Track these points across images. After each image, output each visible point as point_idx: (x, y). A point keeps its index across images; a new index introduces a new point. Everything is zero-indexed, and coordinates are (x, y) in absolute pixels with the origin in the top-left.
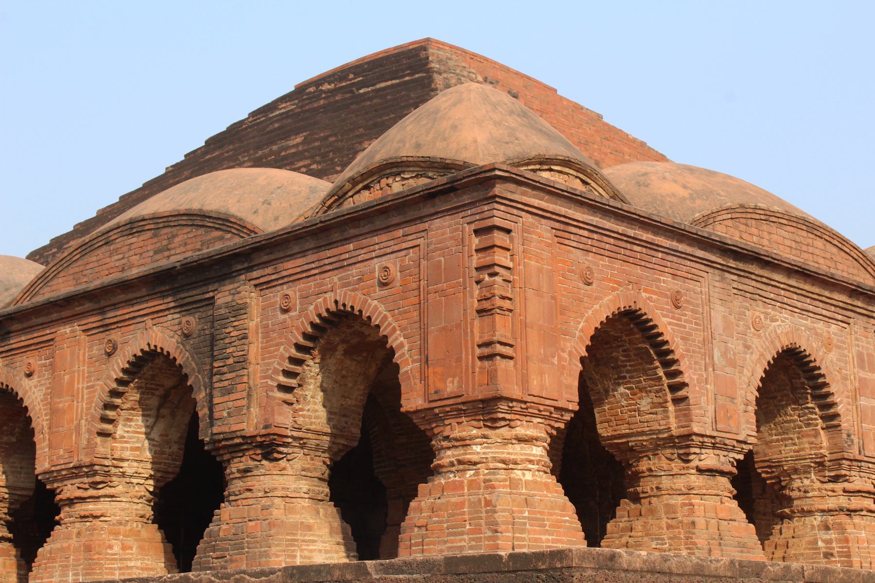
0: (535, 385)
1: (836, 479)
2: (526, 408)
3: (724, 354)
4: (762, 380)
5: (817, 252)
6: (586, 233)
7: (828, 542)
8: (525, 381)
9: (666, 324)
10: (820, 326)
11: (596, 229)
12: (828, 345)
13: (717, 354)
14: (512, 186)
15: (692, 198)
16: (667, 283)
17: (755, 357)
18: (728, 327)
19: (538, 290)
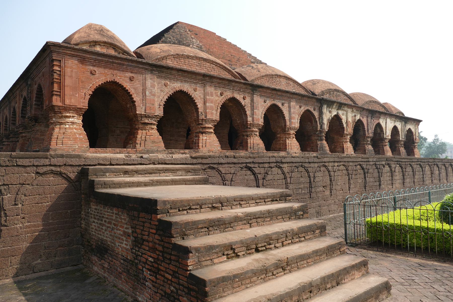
0: (67, 102)
1: (199, 124)
2: (67, 109)
3: (151, 93)
4: (167, 99)
5: (207, 66)
6: (93, 61)
7: (196, 140)
8: (63, 101)
9: (127, 85)
10: (193, 86)
11: (95, 60)
12: (195, 90)
13: (147, 93)
14: (58, 48)
15: (160, 52)
17: (165, 94)
18: (153, 86)
19: (71, 77)
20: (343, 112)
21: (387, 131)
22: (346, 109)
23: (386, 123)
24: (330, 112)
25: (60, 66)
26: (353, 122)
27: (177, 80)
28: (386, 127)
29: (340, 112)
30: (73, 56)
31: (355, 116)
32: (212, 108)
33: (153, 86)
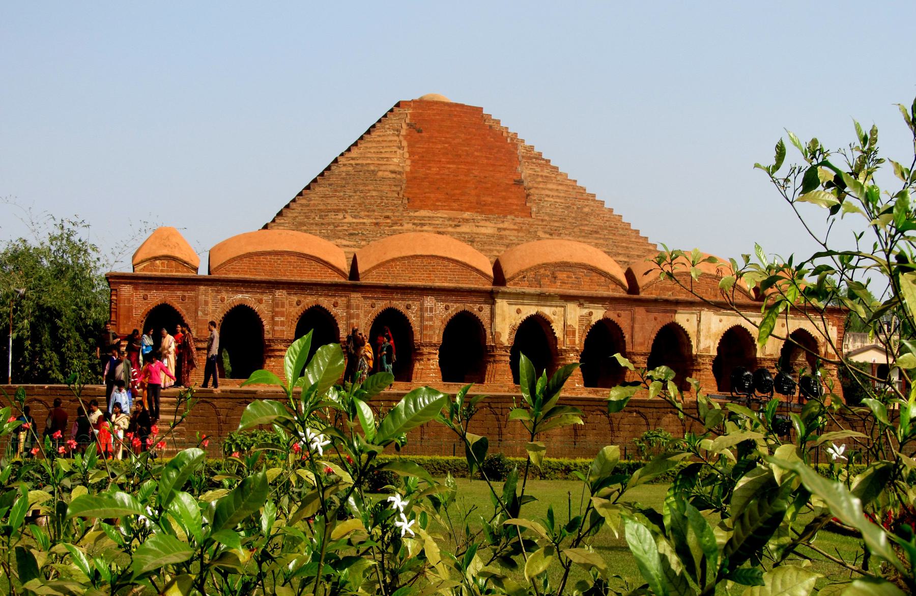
9: (178, 306)
10: (258, 296)
12: (260, 301)
16: (179, 293)
20: (553, 309)
21: (702, 339)
22: (562, 303)
23: (700, 321)
24: (519, 311)
25: (116, 295)
26: (581, 325)
27: (237, 292)
28: (698, 331)
29: (547, 311)
30: (126, 283)
31: (591, 314)
32: (283, 324)
33: (206, 303)
